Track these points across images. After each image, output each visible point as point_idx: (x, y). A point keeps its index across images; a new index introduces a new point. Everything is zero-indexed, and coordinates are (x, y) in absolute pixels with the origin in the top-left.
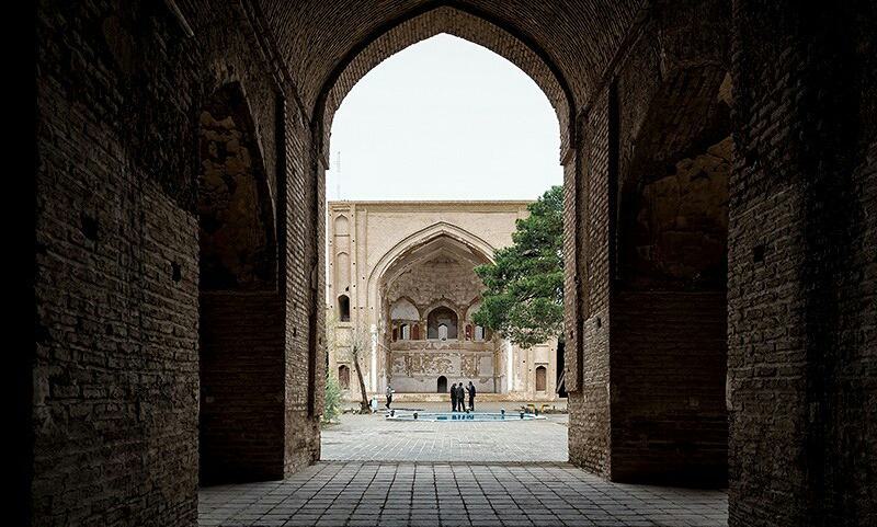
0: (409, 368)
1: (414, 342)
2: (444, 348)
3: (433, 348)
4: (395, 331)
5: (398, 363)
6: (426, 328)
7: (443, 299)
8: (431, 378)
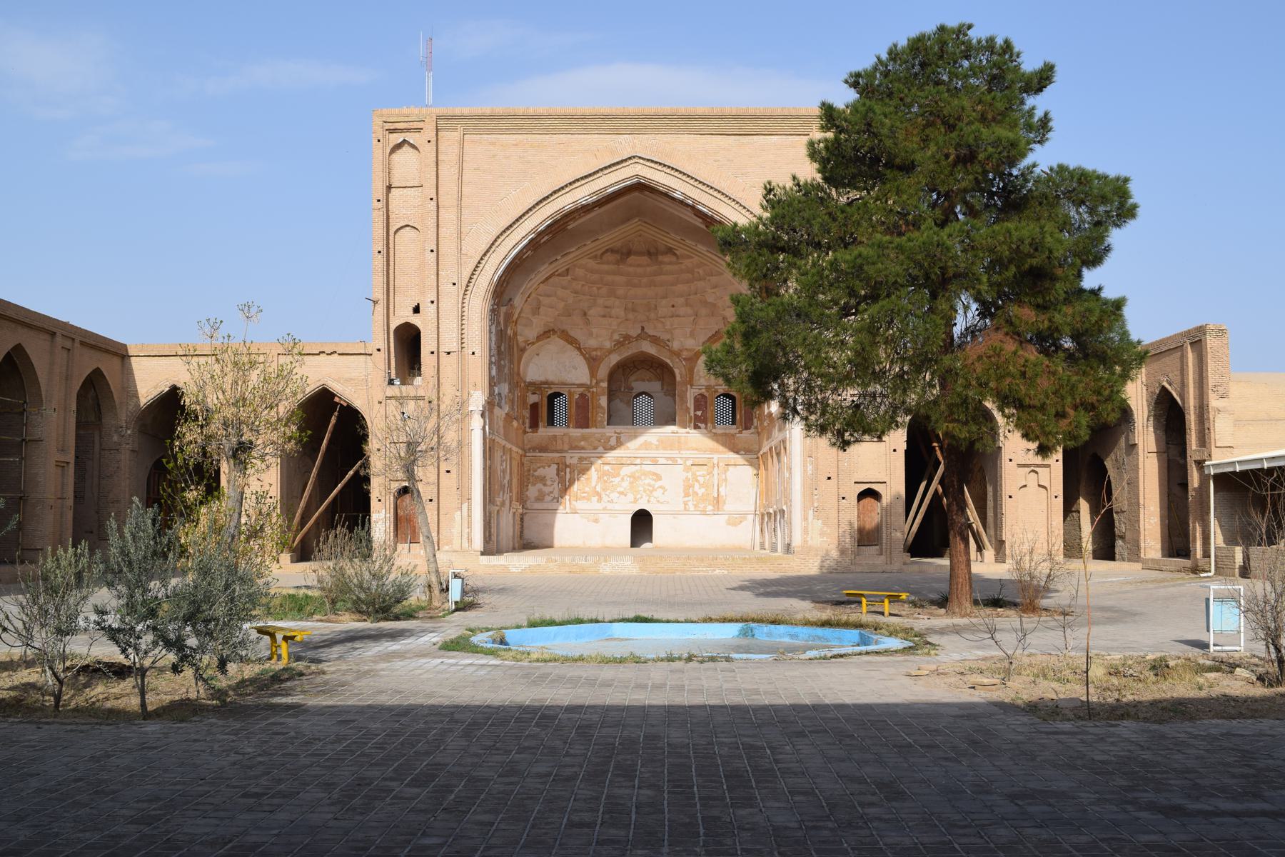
1: (576, 432)
4: (534, 408)
5: (542, 480)
6: (603, 401)
7: (643, 335)
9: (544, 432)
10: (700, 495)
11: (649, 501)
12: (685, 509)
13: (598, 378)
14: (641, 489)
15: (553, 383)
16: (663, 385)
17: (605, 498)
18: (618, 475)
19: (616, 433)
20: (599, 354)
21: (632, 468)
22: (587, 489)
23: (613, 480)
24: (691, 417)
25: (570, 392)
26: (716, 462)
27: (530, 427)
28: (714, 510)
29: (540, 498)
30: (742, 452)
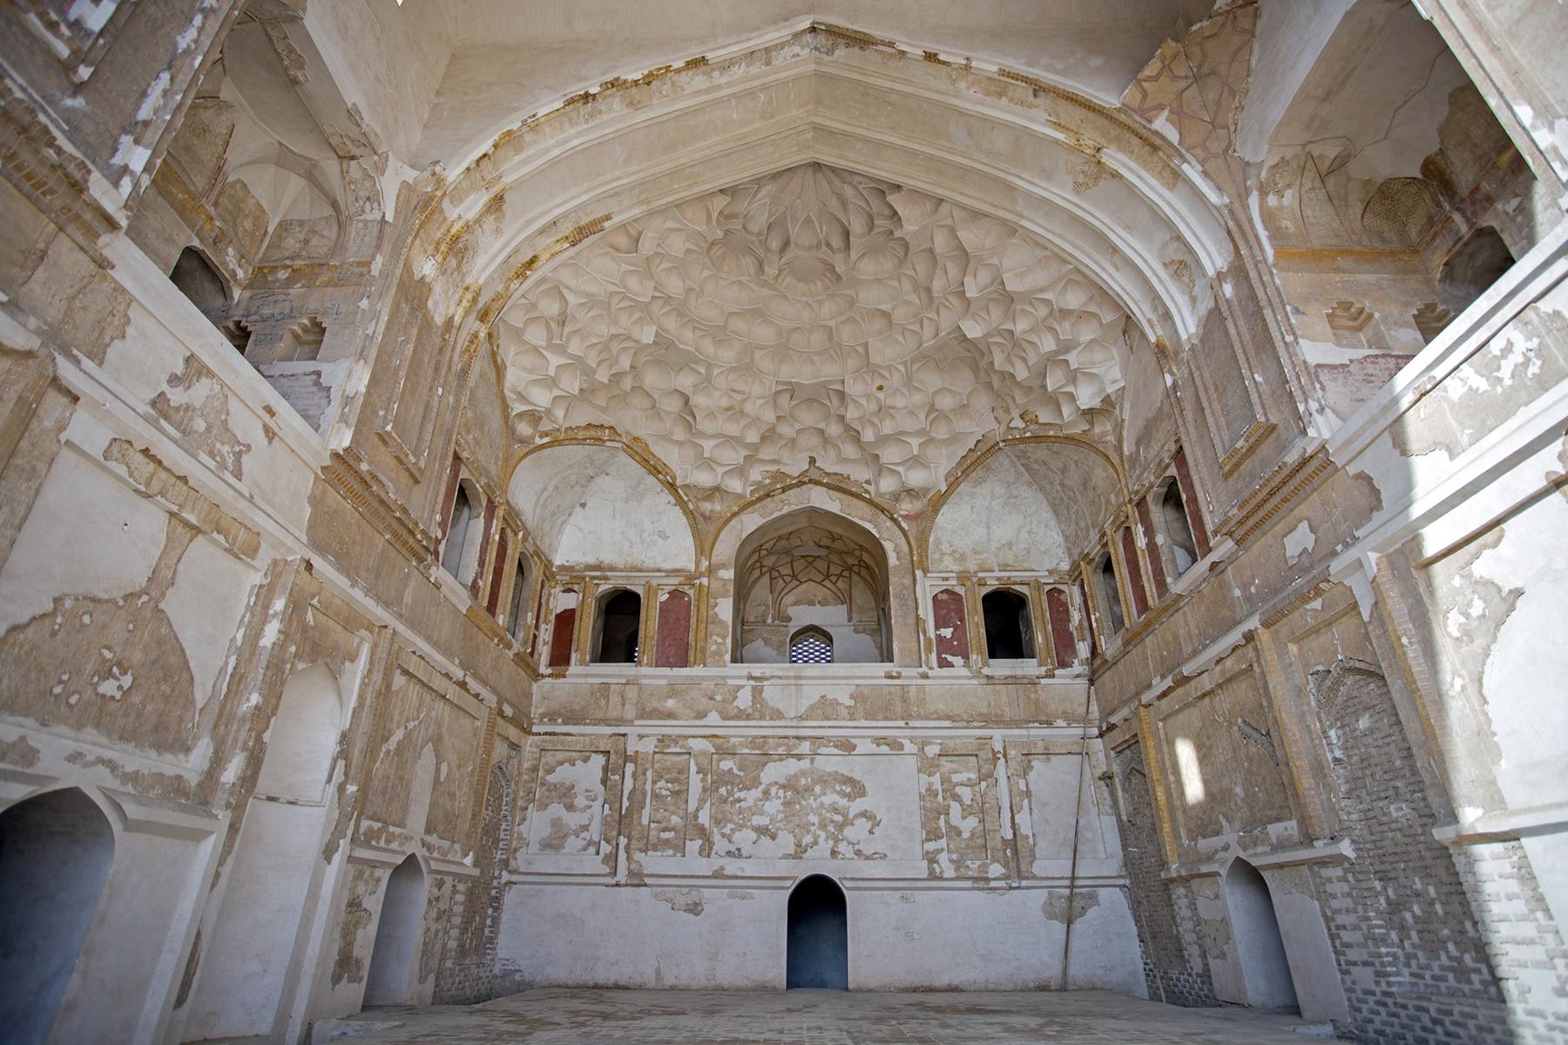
0: (621, 822)
2: (825, 708)
3: (760, 710)
4: (566, 621)
5: (565, 794)
6: (725, 609)
8: (743, 885)
9: (584, 673)
10: (966, 835)
11: (834, 853)
12: (933, 876)
13: (714, 559)
14: (814, 819)
15: (612, 569)
16: (850, 612)
17: (720, 845)
18: (756, 782)
19: (750, 677)
20: (718, 508)
21: (792, 766)
22: (675, 820)
23: (742, 795)
24: (928, 641)
25: (648, 587)
26: (998, 747)
27: (551, 664)
28: (1006, 877)
29: (553, 844)
30: (1060, 723)
